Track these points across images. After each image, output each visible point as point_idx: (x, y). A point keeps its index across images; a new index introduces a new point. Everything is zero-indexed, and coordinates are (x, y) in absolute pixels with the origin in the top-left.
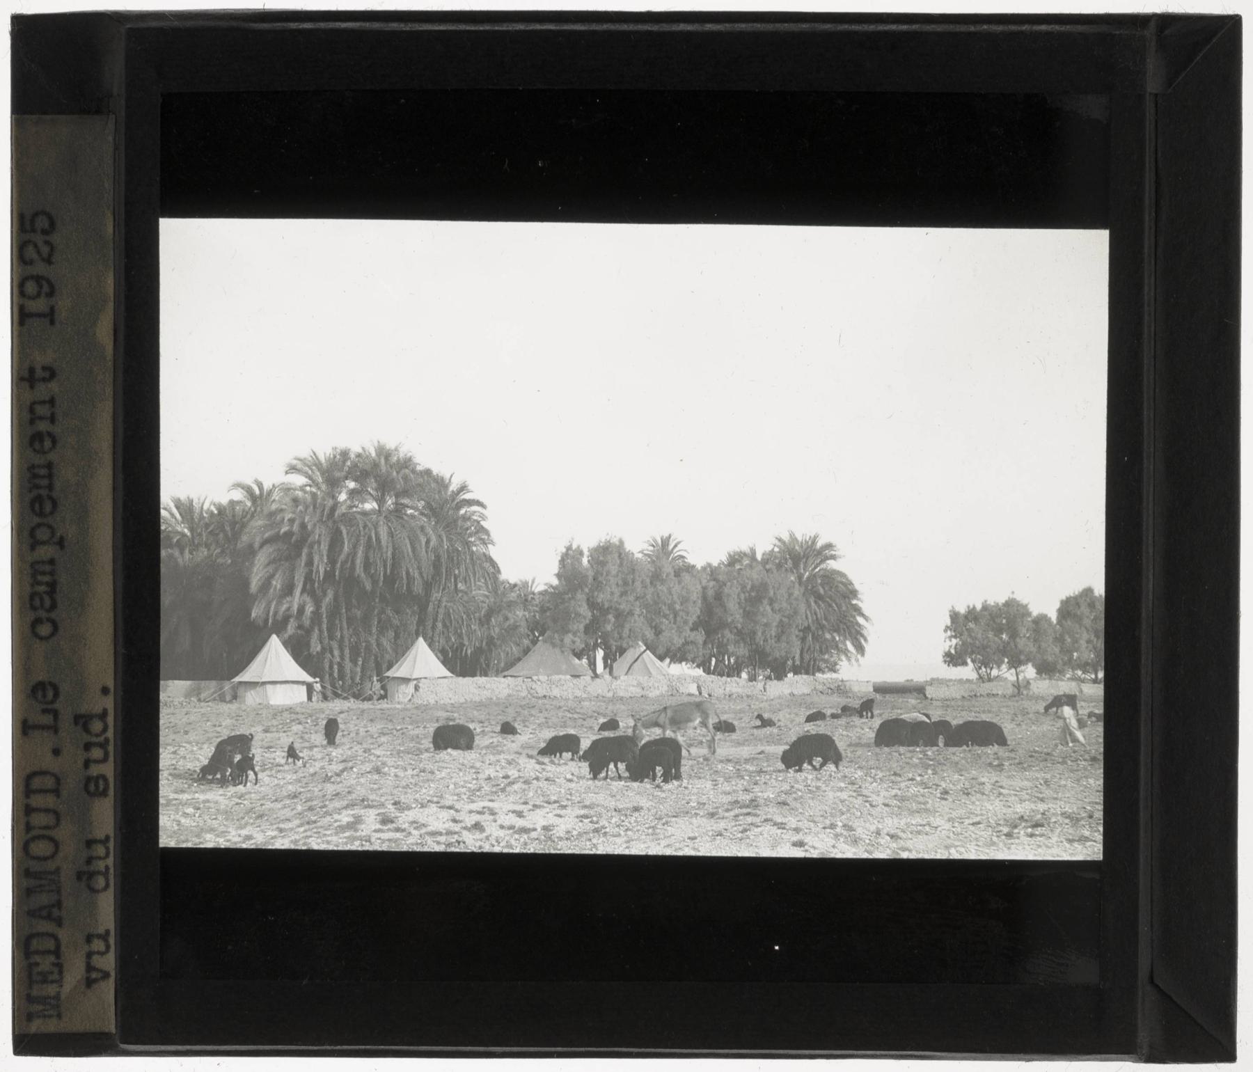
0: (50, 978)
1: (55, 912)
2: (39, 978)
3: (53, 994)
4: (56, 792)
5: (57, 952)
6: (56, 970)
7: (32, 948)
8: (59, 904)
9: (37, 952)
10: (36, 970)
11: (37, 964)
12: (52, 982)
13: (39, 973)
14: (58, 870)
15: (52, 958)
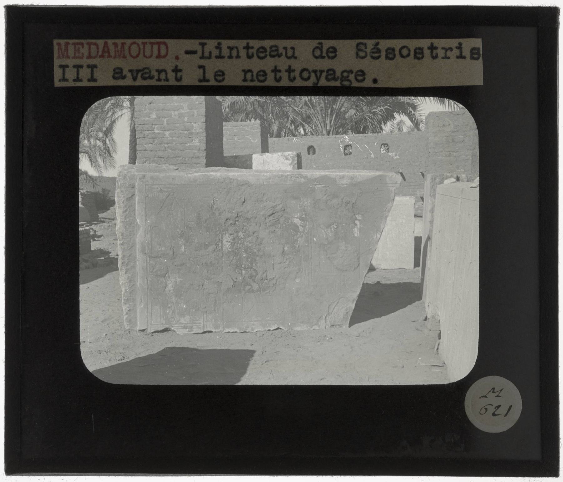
0: (77, 53)
1: (107, 54)
2: (77, 48)
3: (69, 54)
4: (159, 56)
5: (89, 57)
6: (81, 55)
7: (92, 46)
8: (109, 56)
9: (90, 48)
10: (80, 46)
11: (83, 47)
12: (75, 53)
13: (79, 48)
14: (124, 57)
15: (86, 54)
